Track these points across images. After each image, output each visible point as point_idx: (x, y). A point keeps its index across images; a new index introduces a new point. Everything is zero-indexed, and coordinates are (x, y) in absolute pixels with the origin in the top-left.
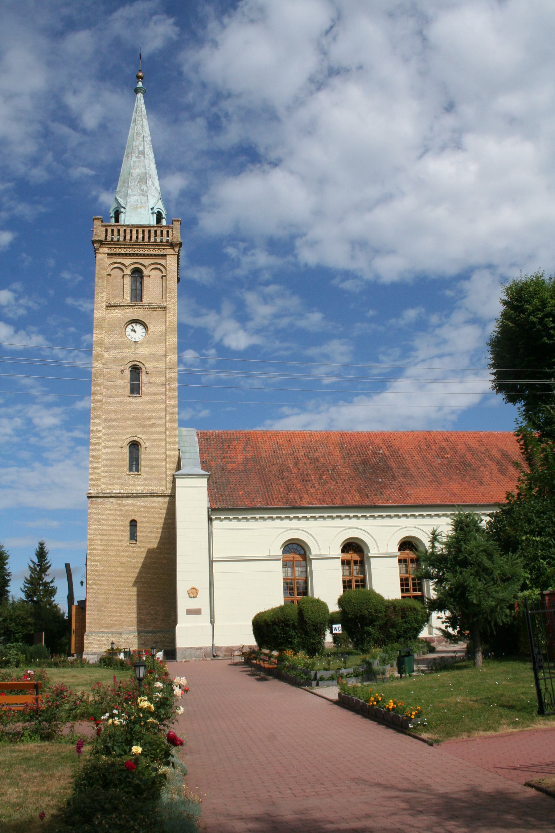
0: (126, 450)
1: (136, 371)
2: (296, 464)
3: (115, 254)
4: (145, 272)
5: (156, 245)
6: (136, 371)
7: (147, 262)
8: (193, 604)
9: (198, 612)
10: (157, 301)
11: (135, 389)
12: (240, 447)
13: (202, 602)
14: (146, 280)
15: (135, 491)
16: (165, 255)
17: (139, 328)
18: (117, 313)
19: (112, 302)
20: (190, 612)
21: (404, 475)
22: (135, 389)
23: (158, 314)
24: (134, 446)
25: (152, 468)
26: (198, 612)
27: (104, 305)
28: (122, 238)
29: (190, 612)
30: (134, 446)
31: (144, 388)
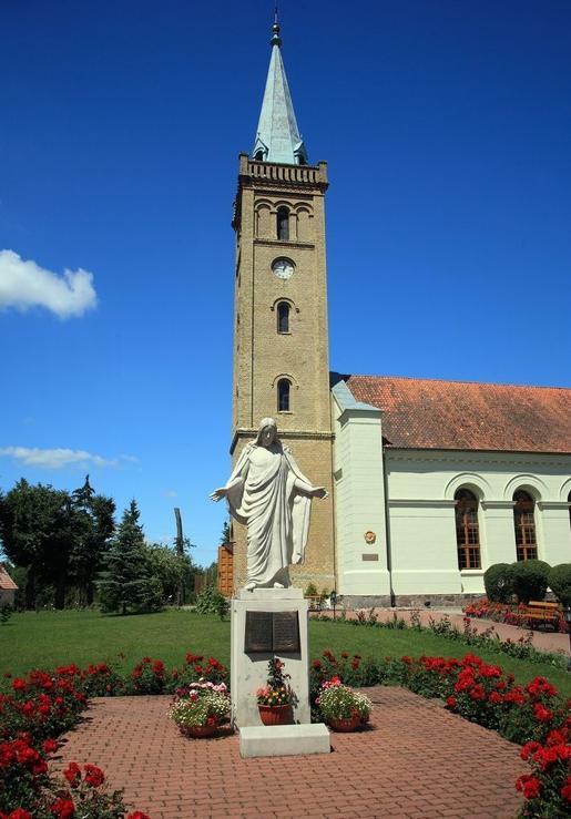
0: (275, 390)
1: (283, 309)
2: (448, 410)
3: (262, 191)
4: (293, 211)
5: (302, 185)
6: (283, 309)
7: (294, 201)
8: (370, 549)
9: (374, 558)
10: (303, 241)
11: (283, 326)
12: (387, 391)
13: (379, 548)
14: (292, 220)
15: (286, 430)
16: (313, 196)
17: (289, 269)
18: (260, 249)
19: (260, 238)
20: (366, 558)
21: (557, 425)
22: (283, 326)
23: (304, 253)
24: (284, 386)
25: (304, 407)
26: (374, 558)
27: (252, 240)
28: (268, 176)
29: (366, 558)
30: (284, 386)
31: (291, 325)
